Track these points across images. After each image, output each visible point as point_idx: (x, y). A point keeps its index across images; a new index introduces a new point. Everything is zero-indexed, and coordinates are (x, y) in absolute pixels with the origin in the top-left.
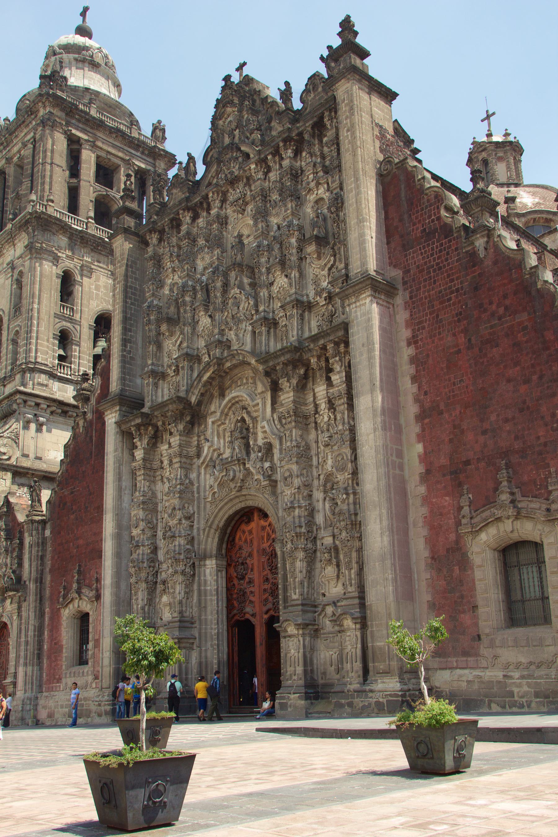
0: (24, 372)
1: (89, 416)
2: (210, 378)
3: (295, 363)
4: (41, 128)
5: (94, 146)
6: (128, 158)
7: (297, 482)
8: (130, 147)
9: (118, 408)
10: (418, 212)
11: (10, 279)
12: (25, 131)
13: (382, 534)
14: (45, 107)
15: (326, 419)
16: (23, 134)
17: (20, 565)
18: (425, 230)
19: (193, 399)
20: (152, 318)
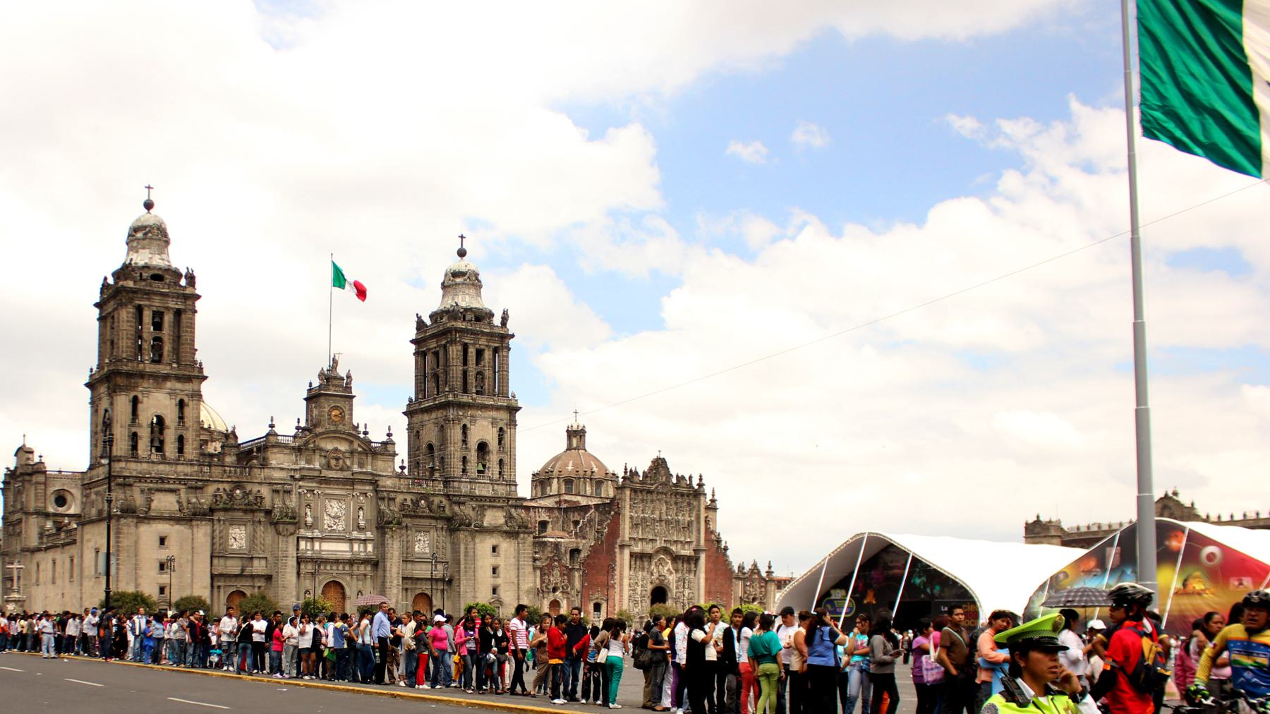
17: (570, 581)
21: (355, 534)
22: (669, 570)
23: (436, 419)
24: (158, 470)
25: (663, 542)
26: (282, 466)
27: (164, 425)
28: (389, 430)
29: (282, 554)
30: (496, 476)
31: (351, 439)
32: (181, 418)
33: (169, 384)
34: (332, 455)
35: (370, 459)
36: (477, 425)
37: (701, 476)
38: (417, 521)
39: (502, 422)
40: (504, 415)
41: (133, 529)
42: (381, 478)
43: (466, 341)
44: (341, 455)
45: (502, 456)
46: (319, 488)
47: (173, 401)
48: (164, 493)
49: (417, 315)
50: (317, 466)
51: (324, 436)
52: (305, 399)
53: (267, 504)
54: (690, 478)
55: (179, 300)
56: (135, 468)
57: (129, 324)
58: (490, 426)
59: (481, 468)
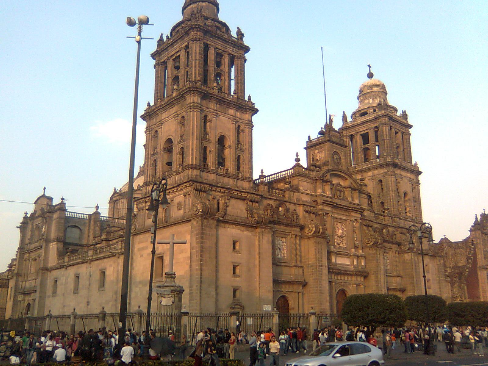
23: (372, 176)
24: (223, 182)
26: (306, 192)
27: (224, 146)
29: (319, 263)
30: (414, 218)
31: (347, 177)
34: (338, 188)
39: (413, 181)
40: (412, 176)
41: (213, 231)
43: (392, 125)
44: (342, 189)
46: (332, 212)
47: (234, 125)
48: (236, 200)
49: (344, 112)
51: (332, 173)
52: (305, 148)
53: (302, 222)
55: (235, 49)
56: (206, 178)
57: (201, 56)
58: (408, 183)
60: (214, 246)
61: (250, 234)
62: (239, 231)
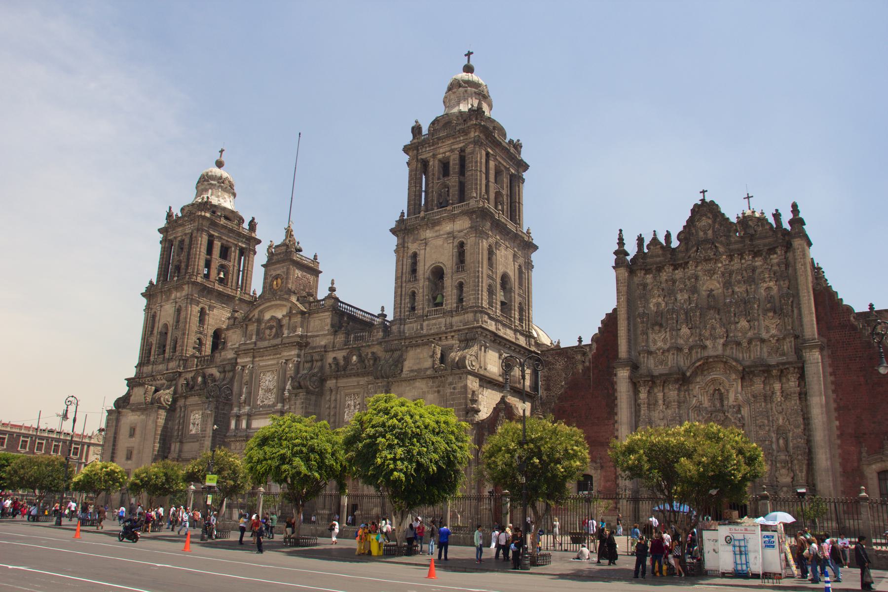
0: (476, 312)
1: (587, 364)
2: (700, 365)
3: (764, 371)
4: (473, 146)
5: (495, 160)
6: (508, 167)
7: (767, 428)
8: (509, 159)
9: (629, 368)
10: (836, 313)
11: (451, 245)
12: (452, 141)
13: (827, 460)
14: (475, 133)
15: (779, 400)
16: (450, 142)
18: (840, 324)
19: (688, 374)
20: (645, 320)
21: (279, 406)
22: (736, 399)
25: (720, 348)
26: (234, 346)
28: (333, 283)
32: (178, 321)
33: (173, 296)
34: (268, 324)
35: (298, 319)
36: (428, 249)
37: (795, 207)
38: (342, 382)
39: (462, 234)
40: (463, 224)
42: (315, 339)
43: (423, 157)
44: (275, 324)
45: (462, 277)
46: (253, 362)
50: (254, 340)
54: (777, 216)
58: (446, 245)
59: (438, 300)
60: (113, 435)
61: (144, 417)
62: (136, 416)
